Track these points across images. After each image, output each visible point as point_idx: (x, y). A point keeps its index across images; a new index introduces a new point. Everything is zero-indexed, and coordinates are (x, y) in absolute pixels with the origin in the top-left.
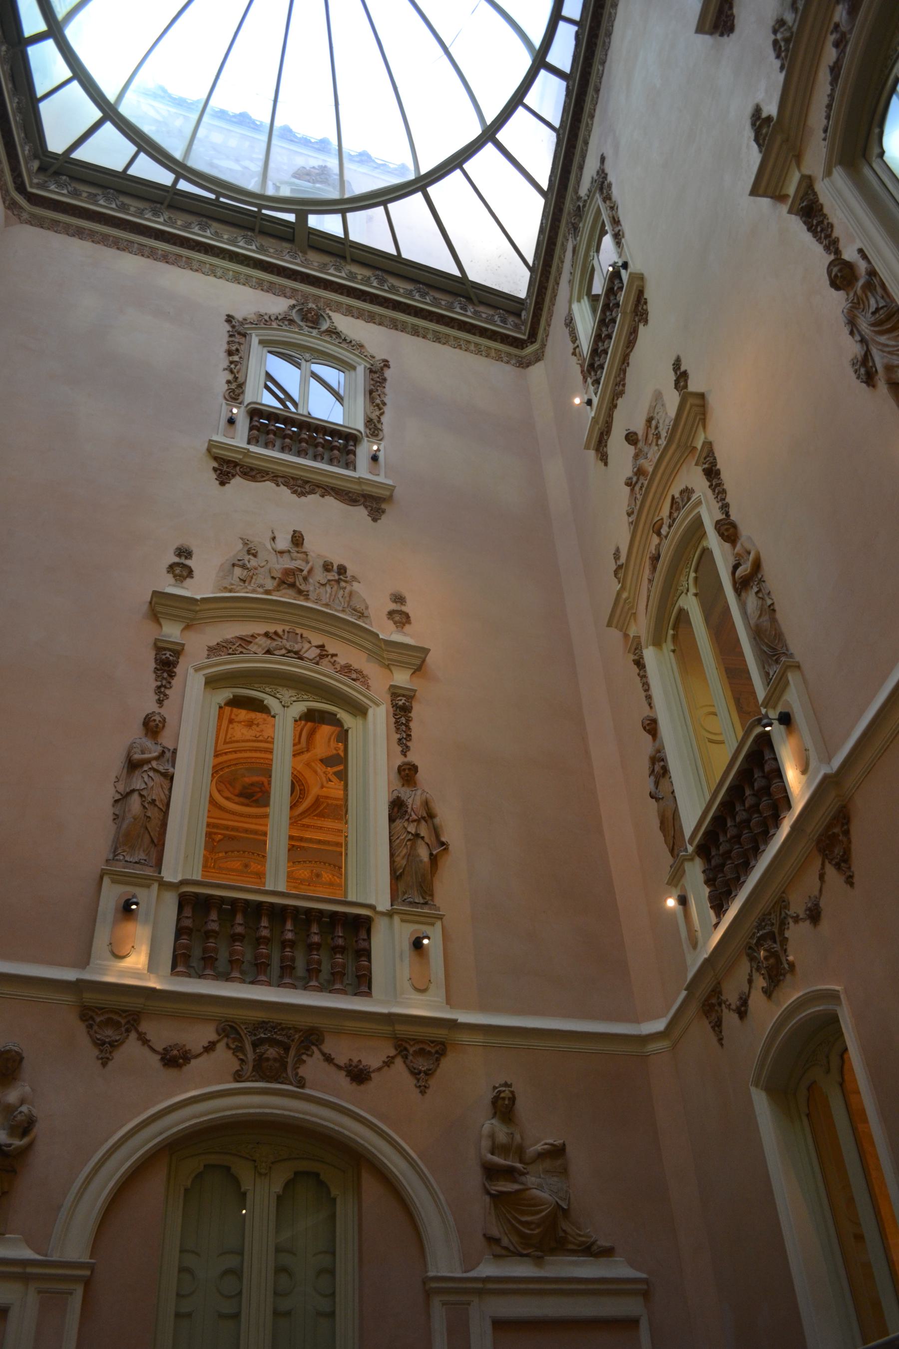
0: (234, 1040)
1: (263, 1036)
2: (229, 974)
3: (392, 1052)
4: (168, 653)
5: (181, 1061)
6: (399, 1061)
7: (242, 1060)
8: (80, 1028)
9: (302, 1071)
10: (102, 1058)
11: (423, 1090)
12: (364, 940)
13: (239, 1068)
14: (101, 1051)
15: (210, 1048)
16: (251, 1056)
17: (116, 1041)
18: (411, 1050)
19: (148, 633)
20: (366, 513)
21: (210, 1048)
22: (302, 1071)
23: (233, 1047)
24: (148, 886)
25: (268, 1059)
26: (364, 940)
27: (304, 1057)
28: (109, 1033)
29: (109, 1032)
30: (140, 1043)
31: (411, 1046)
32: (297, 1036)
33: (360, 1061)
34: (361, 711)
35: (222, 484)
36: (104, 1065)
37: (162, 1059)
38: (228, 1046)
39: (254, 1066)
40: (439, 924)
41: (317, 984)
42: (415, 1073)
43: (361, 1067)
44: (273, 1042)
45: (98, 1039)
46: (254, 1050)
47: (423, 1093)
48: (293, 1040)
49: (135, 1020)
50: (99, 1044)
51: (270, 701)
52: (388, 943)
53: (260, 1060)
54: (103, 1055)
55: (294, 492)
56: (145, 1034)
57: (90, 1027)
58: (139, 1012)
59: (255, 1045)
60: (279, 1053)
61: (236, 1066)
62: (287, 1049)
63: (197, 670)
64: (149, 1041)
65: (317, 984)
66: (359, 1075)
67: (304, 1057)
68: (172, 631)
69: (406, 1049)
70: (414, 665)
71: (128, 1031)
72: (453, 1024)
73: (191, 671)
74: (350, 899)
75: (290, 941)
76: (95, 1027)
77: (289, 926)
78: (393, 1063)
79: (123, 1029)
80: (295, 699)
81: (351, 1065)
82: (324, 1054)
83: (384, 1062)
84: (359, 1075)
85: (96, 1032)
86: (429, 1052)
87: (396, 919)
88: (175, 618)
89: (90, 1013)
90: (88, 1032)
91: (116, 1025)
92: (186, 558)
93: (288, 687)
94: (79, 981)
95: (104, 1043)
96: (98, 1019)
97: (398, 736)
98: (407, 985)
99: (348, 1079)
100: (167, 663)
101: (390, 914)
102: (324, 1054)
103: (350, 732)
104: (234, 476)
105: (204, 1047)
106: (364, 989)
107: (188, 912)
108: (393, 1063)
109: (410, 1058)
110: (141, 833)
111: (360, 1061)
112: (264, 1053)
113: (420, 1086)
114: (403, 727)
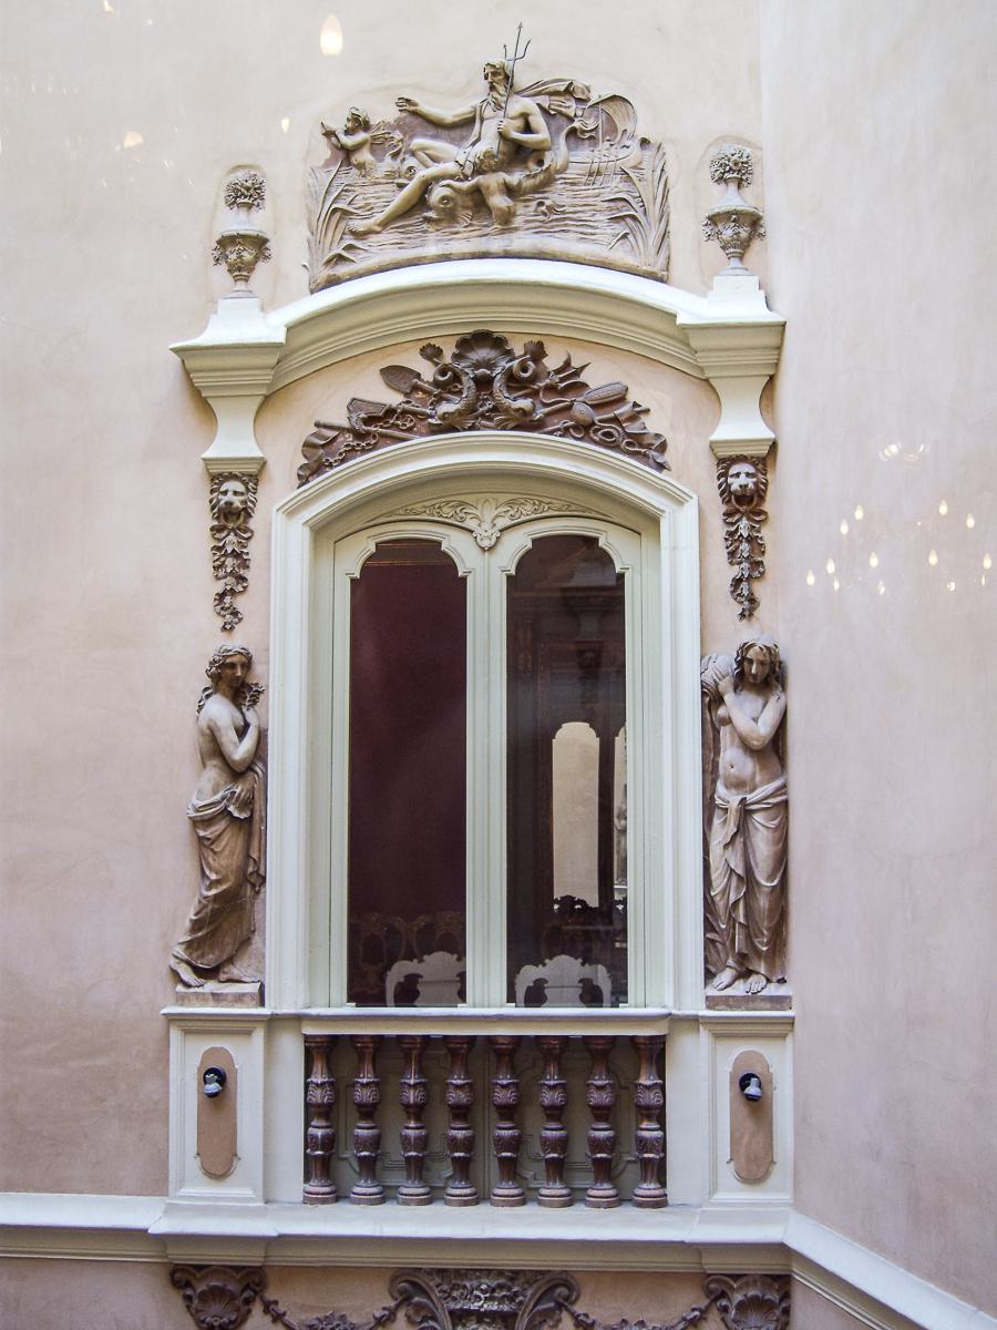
6: (714, 1315)
8: (176, 1300)
18: (738, 1297)
30: (268, 1319)
32: (529, 1292)
38: (409, 1318)
51: (457, 546)
52: (696, 1089)
56: (276, 1303)
57: (188, 1298)
71: (248, 1301)
76: (196, 1301)
78: (705, 1319)
82: (575, 1317)
90: (188, 1307)
97: (735, 571)
102: (575, 1317)
106: (649, 1189)
107: (318, 1079)
108: (705, 1319)
110: (223, 928)
114: (745, 546)
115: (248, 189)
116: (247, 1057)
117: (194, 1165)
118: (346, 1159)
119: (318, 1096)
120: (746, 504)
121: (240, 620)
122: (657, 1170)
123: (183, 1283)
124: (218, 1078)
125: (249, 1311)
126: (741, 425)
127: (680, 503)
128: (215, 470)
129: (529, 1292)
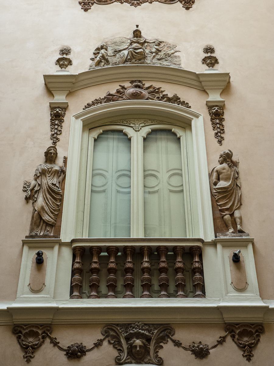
0: (113, 337)
1: (131, 331)
2: (107, 294)
3: (223, 334)
4: (58, 110)
5: (79, 354)
6: (229, 339)
7: (120, 350)
9: (161, 353)
10: (27, 357)
11: (249, 358)
12: (198, 262)
13: (118, 355)
14: (26, 353)
15: (98, 345)
16: (125, 346)
17: (36, 345)
18: (237, 332)
19: (46, 102)
20: (181, 5)
21: (98, 345)
22: (161, 353)
23: (113, 342)
24: (52, 248)
25: (136, 347)
26: (198, 262)
27: (162, 344)
28: (31, 340)
29: (31, 340)
30: (52, 345)
31: (237, 329)
33: (200, 342)
34: (186, 125)
35: (86, 10)
36: (28, 361)
37: (67, 354)
38: (109, 341)
39: (128, 353)
40: (250, 247)
41: (166, 293)
42: (242, 347)
43: (201, 346)
44: (138, 336)
45: (24, 345)
46: (127, 342)
47: (249, 360)
48: (153, 333)
49: (48, 331)
50: (25, 348)
53: (131, 348)
54: (28, 355)
55: (132, 4)
57: (19, 338)
58: (51, 324)
59: (127, 339)
60: (143, 342)
61: (115, 353)
62: (149, 340)
63: (77, 117)
64: (58, 343)
65: (166, 293)
66: (201, 353)
67: (162, 344)
68: (60, 98)
69: (233, 331)
70: (222, 89)
71: (44, 338)
72: (266, 309)
73: (74, 118)
74: (188, 237)
75: (147, 268)
76: (22, 337)
77: (146, 259)
79: (40, 337)
80: (143, 125)
81: (194, 346)
83: (218, 341)
84: (201, 353)
85: (22, 341)
86: (250, 331)
87: (219, 246)
88: (61, 89)
89: (19, 329)
91: (35, 335)
92: (67, 54)
93: (138, 119)
94: (10, 311)
95: (28, 347)
96: (24, 332)
98: (231, 288)
99: (193, 356)
100: (57, 116)
101: (214, 244)
103: (181, 138)
104: (92, 4)
105: (94, 344)
107: (78, 260)
109: (237, 337)
111: (200, 342)
112: (133, 343)
113: (246, 356)
115: (66, 50)
116: (51, 257)
117: (27, 289)
118: (85, 293)
119: (77, 266)
120: (217, 115)
121: (59, 141)
122: (202, 288)
123: (17, 331)
124: (40, 261)
125: (43, 342)
126: (215, 97)
127: (197, 116)
128: (53, 106)
129: (156, 331)
